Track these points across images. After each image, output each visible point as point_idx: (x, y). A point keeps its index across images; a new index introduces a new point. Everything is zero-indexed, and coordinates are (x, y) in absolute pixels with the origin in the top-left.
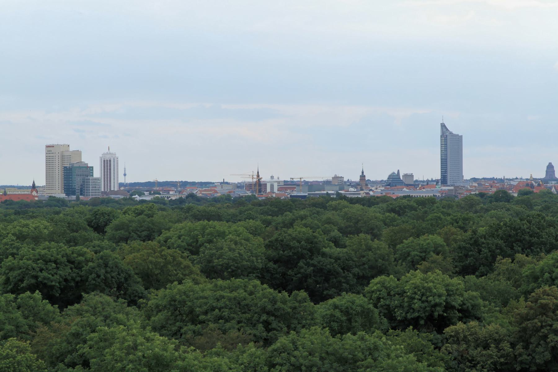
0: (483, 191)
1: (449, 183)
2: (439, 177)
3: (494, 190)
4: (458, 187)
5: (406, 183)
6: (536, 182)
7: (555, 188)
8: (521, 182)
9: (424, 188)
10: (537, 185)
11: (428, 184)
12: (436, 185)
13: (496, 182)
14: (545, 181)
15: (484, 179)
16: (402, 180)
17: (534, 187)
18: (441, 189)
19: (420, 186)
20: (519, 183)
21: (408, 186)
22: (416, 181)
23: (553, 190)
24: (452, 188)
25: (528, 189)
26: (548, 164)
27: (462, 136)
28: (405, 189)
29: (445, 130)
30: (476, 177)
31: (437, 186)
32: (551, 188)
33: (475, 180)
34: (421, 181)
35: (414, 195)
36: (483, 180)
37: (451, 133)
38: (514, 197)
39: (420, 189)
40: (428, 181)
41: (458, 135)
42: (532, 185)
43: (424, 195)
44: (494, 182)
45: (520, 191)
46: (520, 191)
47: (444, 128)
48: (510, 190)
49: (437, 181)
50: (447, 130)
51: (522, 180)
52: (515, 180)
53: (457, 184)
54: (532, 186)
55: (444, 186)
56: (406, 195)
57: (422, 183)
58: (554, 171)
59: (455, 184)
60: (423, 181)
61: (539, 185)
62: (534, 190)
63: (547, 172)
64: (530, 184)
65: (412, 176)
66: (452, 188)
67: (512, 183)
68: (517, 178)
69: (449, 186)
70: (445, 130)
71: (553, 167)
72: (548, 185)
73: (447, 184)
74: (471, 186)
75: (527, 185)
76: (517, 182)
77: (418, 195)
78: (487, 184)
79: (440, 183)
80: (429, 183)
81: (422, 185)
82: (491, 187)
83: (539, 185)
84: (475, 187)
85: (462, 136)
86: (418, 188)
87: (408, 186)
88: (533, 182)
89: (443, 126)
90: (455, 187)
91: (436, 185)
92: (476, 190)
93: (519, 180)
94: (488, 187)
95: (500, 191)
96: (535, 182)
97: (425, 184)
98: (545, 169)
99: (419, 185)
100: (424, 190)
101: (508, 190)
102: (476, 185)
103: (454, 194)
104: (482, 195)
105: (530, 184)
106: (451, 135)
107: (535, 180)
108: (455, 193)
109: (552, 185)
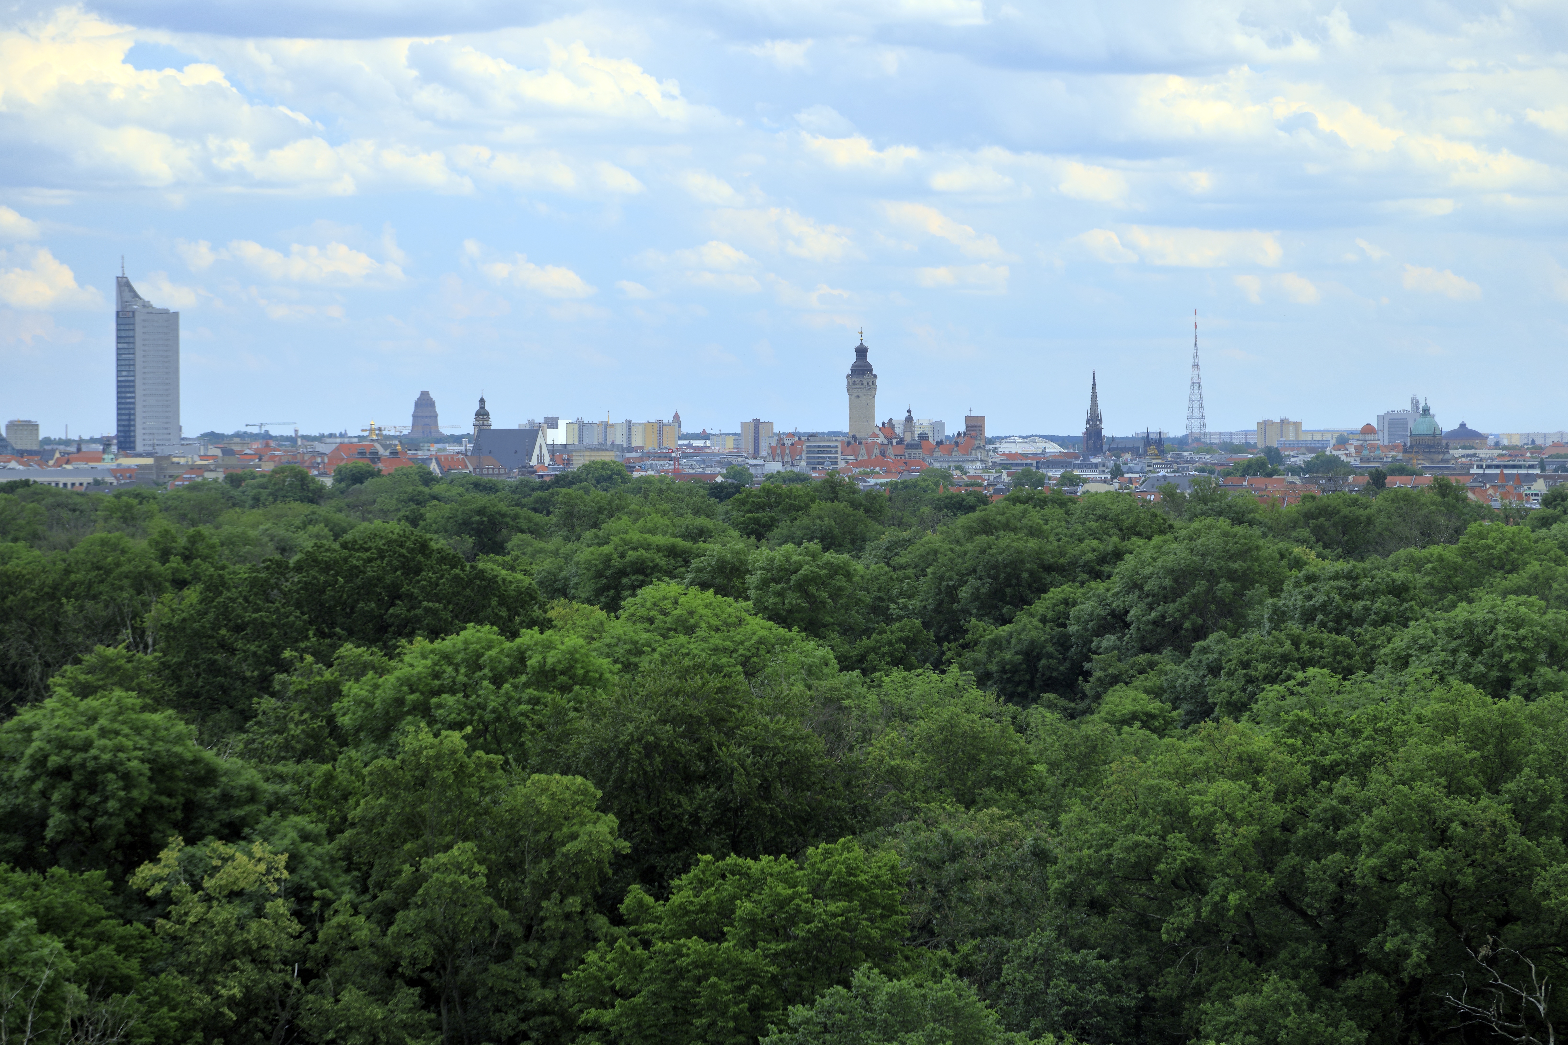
0: (234, 471)
1: (139, 449)
2: (110, 429)
3: (268, 467)
4: (168, 457)
5: (18, 447)
6: (385, 447)
7: (438, 464)
8: (344, 445)
9: (67, 463)
10: (387, 453)
11: (79, 450)
12: (104, 451)
13: (273, 444)
14: (411, 442)
15: (238, 435)
16: (4, 439)
17: (379, 459)
18: (119, 465)
19: (57, 455)
20: (337, 449)
21: (21, 454)
22: (47, 441)
23: (434, 467)
24: (150, 461)
25: (362, 463)
26: (418, 395)
27: (176, 314)
28: (13, 464)
29: (127, 296)
30: (217, 431)
31: (105, 456)
32: (425, 461)
33: (212, 438)
34: (61, 442)
35: (39, 479)
36: (237, 440)
37: (146, 305)
38: (322, 487)
39: (58, 464)
40: (80, 442)
41: (165, 312)
42: (375, 453)
43: (69, 481)
44: (267, 446)
45: (339, 472)
46: (339, 472)
47: (126, 289)
48: (314, 468)
49: (106, 443)
50: (136, 296)
51: (346, 440)
52: (328, 440)
53: (167, 451)
54: (375, 457)
55: (127, 456)
56: (17, 479)
57: (62, 447)
58: (436, 416)
59: (158, 449)
60: (67, 442)
61: (394, 454)
62: (380, 466)
63: (415, 416)
64: (368, 451)
65: (31, 427)
66: (150, 461)
67: (320, 447)
68: (331, 436)
69: (140, 455)
70: (127, 296)
71: (432, 404)
72: (420, 453)
73: (134, 448)
74: (202, 457)
75: (362, 454)
76: (334, 446)
77: (52, 479)
78: (247, 451)
79: (114, 448)
80: (84, 448)
81: (64, 454)
82: (260, 460)
83: (394, 454)
84: (214, 457)
85: (176, 314)
86: (51, 462)
87: (21, 454)
88: (378, 446)
89: (124, 285)
90: (159, 459)
91: (104, 451)
92: (217, 467)
93: (338, 440)
94: (252, 460)
95: (282, 471)
96: (382, 445)
97: (73, 449)
98: (412, 409)
99: (53, 452)
100: (69, 467)
101: (309, 468)
102: (218, 452)
103: (154, 477)
104: (234, 480)
105: (368, 451)
106: (146, 310)
107: (385, 440)
108: (158, 476)
109: (429, 453)
